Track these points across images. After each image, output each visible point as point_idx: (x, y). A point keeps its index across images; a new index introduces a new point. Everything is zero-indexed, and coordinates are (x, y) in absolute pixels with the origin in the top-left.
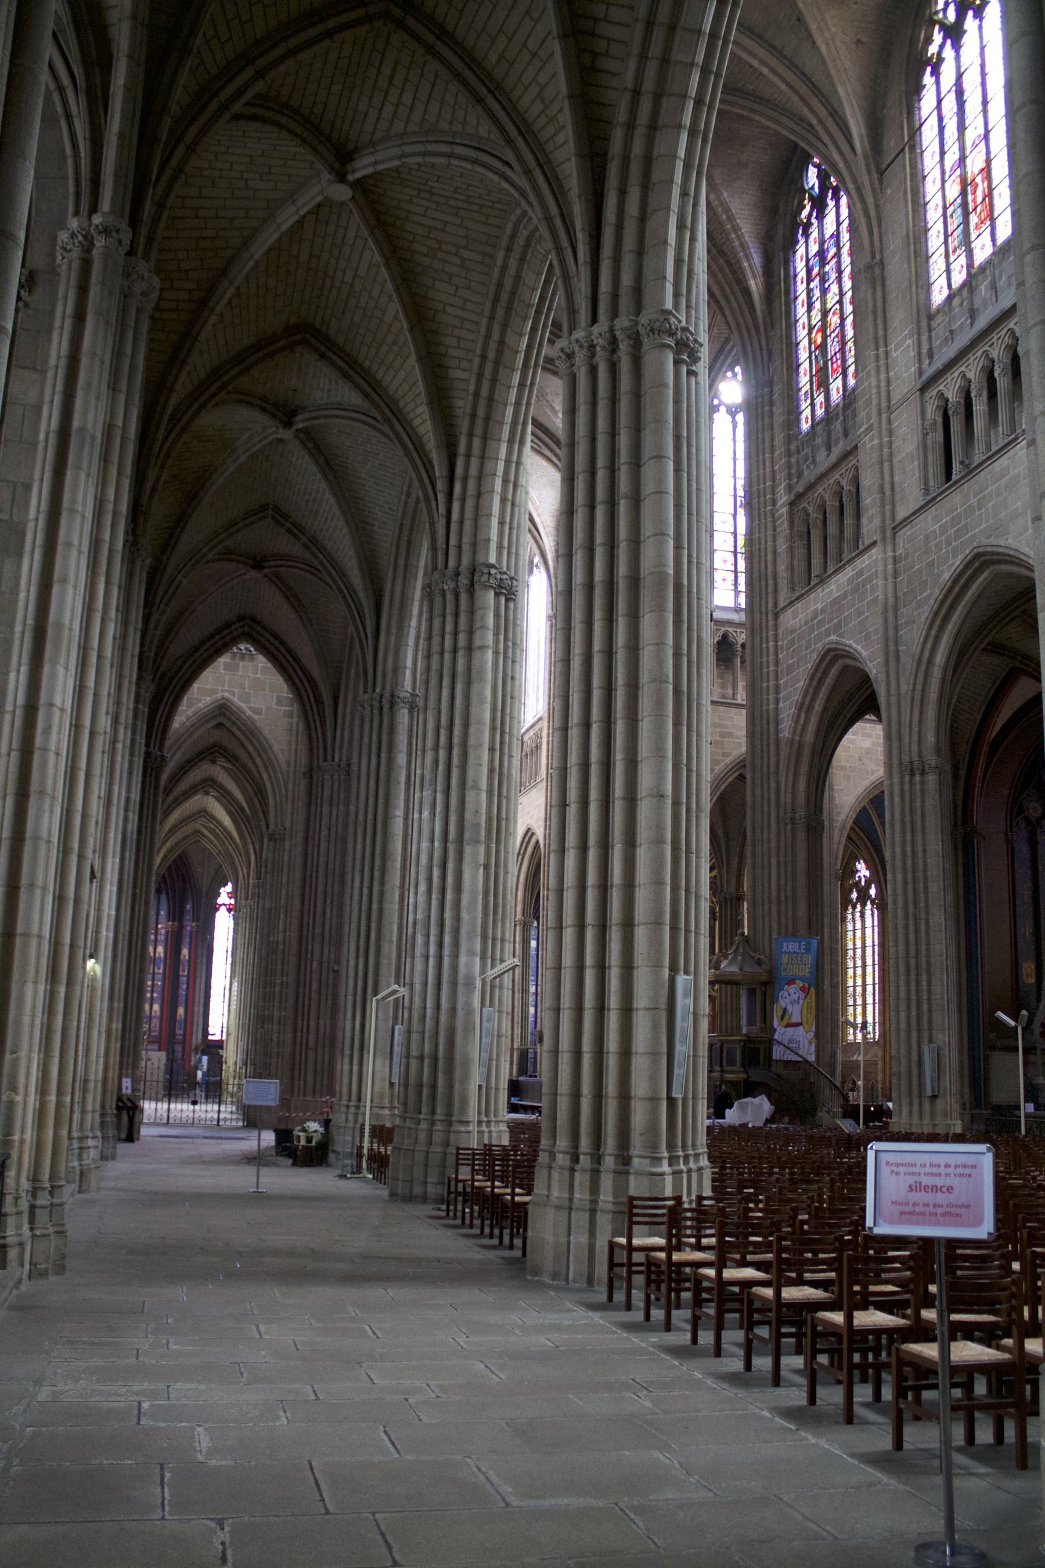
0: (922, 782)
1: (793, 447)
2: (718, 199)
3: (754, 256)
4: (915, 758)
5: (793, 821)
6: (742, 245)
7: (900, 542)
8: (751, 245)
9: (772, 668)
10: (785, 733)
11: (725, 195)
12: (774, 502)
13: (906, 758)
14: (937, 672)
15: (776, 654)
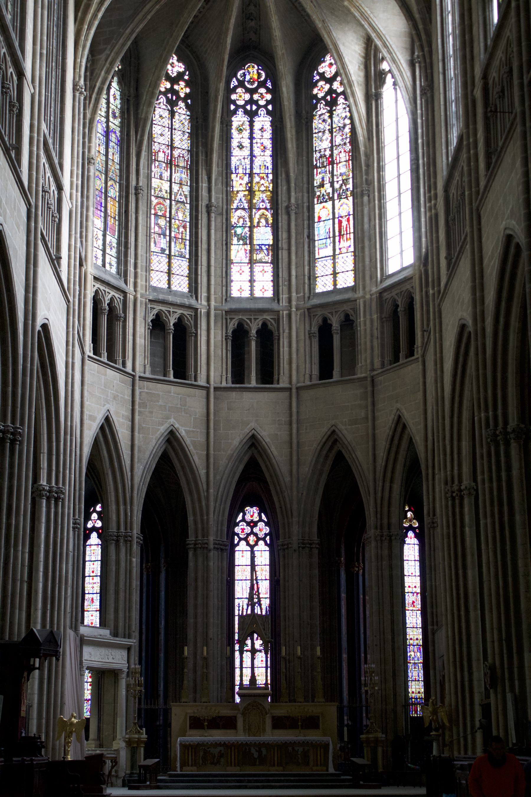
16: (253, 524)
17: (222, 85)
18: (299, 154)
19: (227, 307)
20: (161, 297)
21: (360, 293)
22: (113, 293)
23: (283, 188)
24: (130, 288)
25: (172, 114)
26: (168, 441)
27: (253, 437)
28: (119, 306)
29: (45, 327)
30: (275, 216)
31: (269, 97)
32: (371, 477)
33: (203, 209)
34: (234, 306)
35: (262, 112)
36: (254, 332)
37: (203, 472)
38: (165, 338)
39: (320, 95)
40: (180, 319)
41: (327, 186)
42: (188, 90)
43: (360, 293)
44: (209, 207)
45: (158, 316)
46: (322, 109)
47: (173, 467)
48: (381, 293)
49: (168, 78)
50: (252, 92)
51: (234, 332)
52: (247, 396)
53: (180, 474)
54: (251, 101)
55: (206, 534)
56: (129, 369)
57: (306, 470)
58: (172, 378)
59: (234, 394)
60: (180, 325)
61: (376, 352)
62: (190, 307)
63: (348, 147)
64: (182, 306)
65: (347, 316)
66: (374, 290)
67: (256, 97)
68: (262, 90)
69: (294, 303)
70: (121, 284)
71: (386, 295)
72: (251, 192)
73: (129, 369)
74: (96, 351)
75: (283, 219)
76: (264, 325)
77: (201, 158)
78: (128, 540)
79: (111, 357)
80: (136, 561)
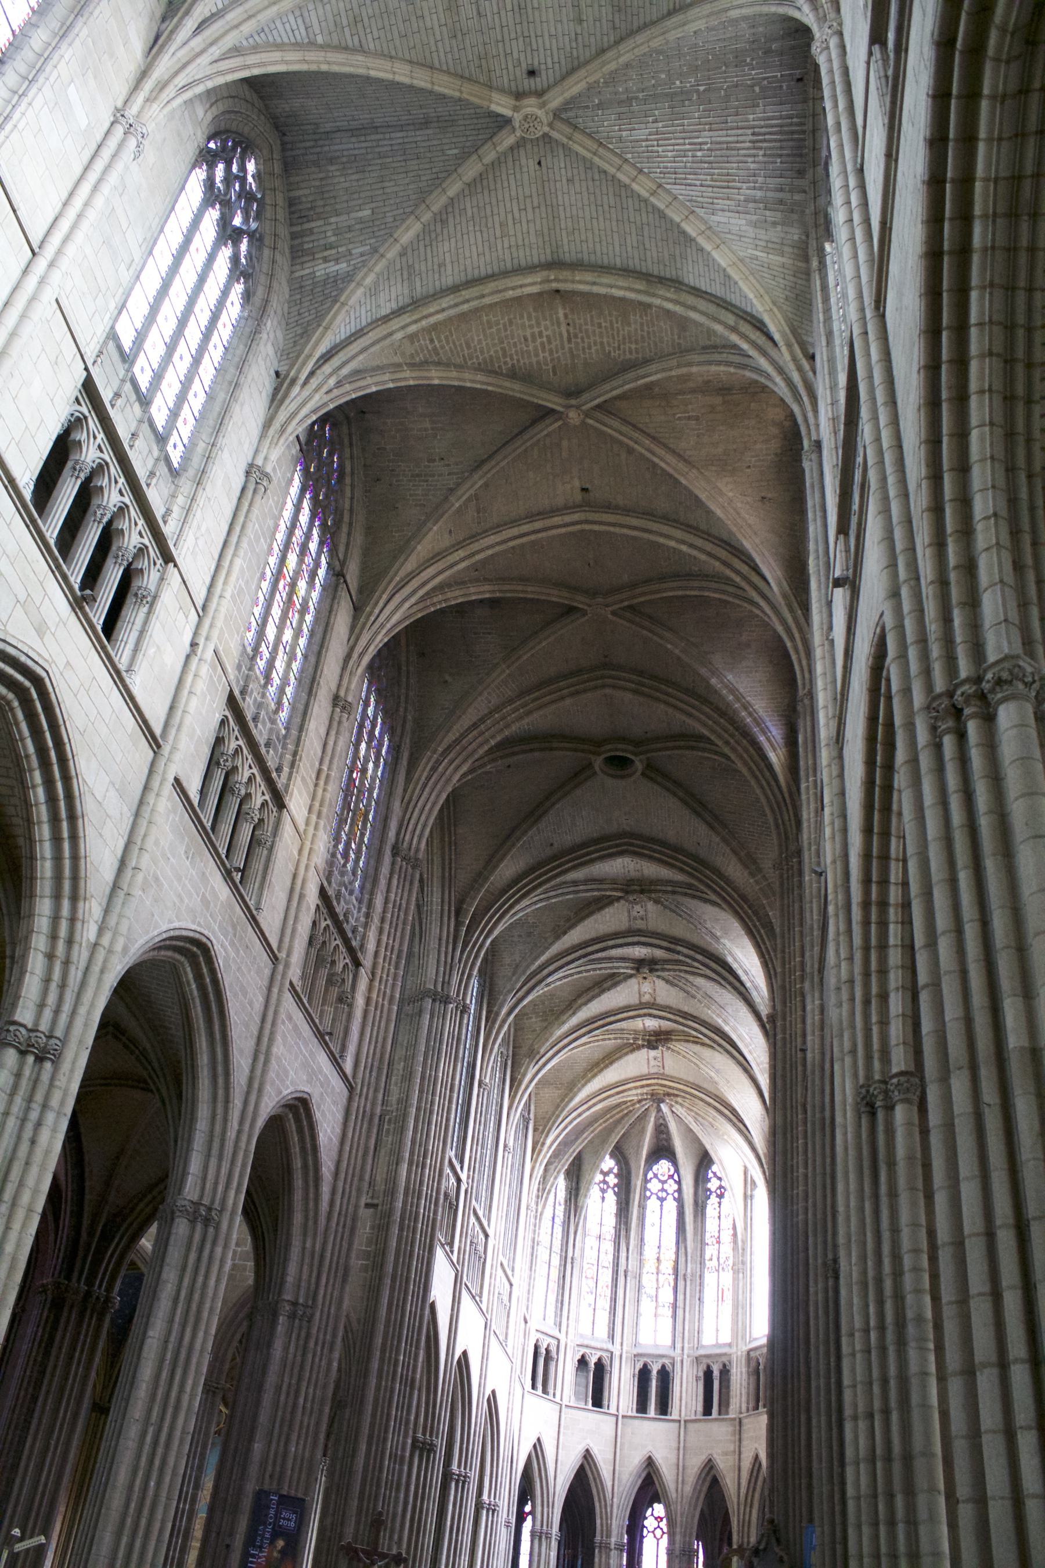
2: (722, 682)
3: (772, 729)
6: (755, 719)
8: (767, 719)
16: (659, 1519)
17: (639, 1183)
18: (695, 1234)
20: (586, 1342)
21: (734, 1350)
22: (550, 1340)
23: (682, 1259)
24: (562, 1337)
25: (603, 1198)
26: (585, 1457)
27: (650, 1458)
29: (493, 1392)
30: (676, 1280)
31: (676, 1187)
32: (735, 1500)
34: (640, 1351)
35: (670, 1198)
36: (654, 1373)
37: (608, 1484)
38: (588, 1371)
39: (713, 1189)
40: (600, 1359)
41: (715, 1262)
42: (616, 1181)
43: (734, 1350)
44: (626, 1272)
45: (583, 1356)
46: (713, 1200)
47: (586, 1475)
48: (749, 1352)
49: (602, 1172)
50: (664, 1182)
51: (640, 1371)
52: (646, 1423)
53: (593, 1485)
54: (663, 1190)
55: (609, 1536)
56: (558, 1399)
57: (688, 1489)
58: (590, 1406)
59: (637, 1422)
60: (600, 1366)
61: (744, 1399)
62: (607, 1351)
63: (731, 1232)
64: (601, 1349)
65: (724, 1365)
66: (745, 1348)
67: (666, 1186)
68: (671, 1181)
69: (686, 1351)
70: (556, 1333)
71: (752, 1354)
72: (658, 1259)
74: (534, 1387)
75: (681, 1283)
76: (663, 1366)
77: (623, 1233)
78: (548, 1537)
79: (545, 1391)
80: (553, 1554)
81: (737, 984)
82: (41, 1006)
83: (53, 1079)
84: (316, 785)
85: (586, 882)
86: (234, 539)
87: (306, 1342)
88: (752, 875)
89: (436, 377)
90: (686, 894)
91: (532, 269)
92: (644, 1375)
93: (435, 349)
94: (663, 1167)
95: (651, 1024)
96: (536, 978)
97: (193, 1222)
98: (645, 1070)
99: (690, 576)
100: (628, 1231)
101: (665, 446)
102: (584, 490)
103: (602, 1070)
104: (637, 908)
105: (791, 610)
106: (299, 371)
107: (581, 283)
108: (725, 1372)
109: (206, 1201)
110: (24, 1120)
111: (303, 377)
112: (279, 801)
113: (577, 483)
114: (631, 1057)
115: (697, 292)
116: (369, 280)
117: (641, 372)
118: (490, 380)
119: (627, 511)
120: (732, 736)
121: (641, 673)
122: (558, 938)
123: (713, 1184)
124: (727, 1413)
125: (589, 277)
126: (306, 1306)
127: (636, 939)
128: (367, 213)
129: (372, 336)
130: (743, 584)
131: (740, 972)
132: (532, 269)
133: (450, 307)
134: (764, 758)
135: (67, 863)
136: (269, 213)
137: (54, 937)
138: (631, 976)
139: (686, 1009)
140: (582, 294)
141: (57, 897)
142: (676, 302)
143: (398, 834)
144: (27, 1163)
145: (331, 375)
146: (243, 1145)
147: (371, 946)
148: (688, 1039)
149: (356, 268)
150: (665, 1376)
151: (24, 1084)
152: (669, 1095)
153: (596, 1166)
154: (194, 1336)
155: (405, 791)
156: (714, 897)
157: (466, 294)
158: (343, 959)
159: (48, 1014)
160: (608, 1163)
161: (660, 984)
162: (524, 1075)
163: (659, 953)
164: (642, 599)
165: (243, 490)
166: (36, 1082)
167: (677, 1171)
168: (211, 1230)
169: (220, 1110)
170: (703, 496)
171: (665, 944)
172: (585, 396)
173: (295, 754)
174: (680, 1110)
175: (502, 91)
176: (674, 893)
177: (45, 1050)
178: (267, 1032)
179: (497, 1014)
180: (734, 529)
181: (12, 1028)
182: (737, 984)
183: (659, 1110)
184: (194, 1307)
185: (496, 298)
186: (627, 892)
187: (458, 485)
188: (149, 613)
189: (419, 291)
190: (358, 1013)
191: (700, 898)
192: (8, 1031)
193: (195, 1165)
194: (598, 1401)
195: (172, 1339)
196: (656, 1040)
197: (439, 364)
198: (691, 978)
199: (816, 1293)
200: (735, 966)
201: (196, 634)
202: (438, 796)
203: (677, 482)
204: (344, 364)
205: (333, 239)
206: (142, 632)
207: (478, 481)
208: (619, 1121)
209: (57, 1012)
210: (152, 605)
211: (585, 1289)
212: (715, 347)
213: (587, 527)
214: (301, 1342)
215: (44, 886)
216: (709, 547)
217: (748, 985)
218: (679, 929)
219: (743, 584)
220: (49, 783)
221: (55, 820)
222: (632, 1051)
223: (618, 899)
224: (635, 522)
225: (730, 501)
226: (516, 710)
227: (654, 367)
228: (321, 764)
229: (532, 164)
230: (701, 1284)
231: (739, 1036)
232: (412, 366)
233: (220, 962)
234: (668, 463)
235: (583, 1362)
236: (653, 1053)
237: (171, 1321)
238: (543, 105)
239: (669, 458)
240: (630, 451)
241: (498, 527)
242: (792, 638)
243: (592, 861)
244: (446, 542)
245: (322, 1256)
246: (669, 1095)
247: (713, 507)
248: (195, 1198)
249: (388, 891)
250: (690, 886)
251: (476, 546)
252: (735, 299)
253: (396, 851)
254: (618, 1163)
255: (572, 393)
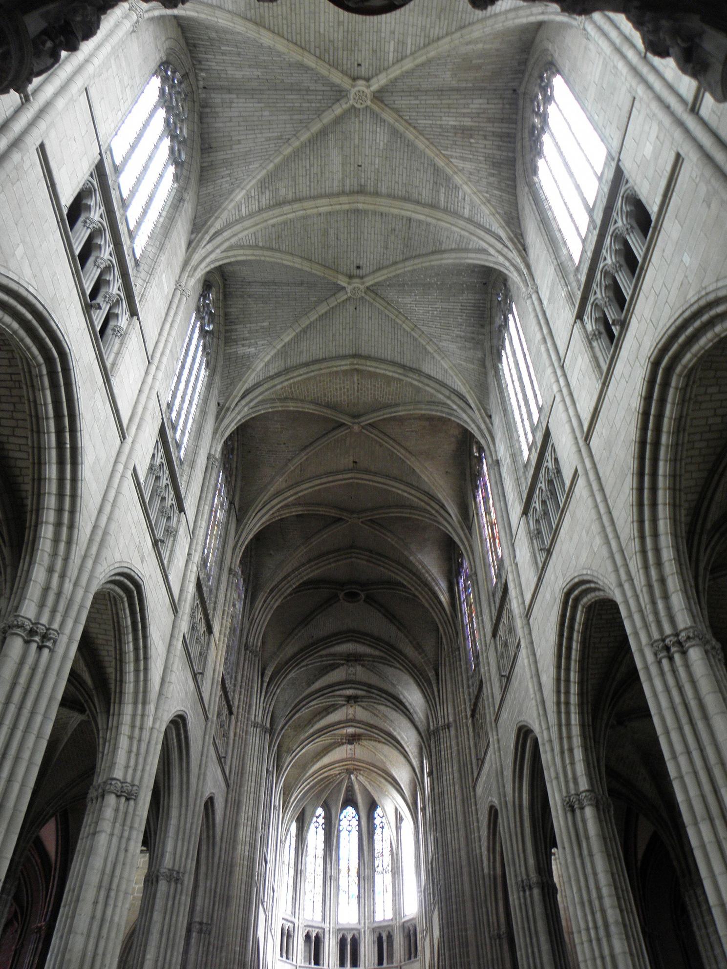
0: (531, 896)
1: (470, 683)
4: (525, 877)
5: (499, 936)
7: (500, 730)
9: (475, 824)
10: (486, 871)
11: (419, 556)
12: (466, 718)
13: (519, 879)
14: (526, 813)
15: (477, 814)
18: (369, 851)
19: (337, 927)
20: (310, 924)
21: (394, 922)
22: (289, 924)
23: (362, 868)
24: (296, 921)
28: (291, 930)
30: (359, 880)
33: (328, 878)
34: (340, 927)
36: (349, 940)
40: (317, 934)
44: (331, 877)
45: (308, 933)
46: (378, 831)
51: (341, 940)
56: (294, 963)
62: (321, 928)
65: (389, 933)
67: (351, 823)
70: (292, 919)
73: (294, 963)
74: (281, 956)
76: (354, 936)
77: (328, 853)
79: (287, 958)
81: (405, 710)
82: (127, 767)
83: (135, 810)
84: (223, 619)
85: (326, 656)
86: (204, 495)
87: (208, 948)
88: (420, 654)
89: (292, 406)
90: (380, 663)
91: (344, 357)
92: (342, 943)
93: (292, 392)
94: (350, 811)
95: (351, 730)
96: (296, 708)
97: (169, 882)
98: (344, 756)
99: (403, 506)
100: (331, 851)
101: (399, 444)
102: (355, 462)
103: (322, 757)
104: (351, 669)
105: (463, 530)
106: (231, 404)
107: (371, 367)
108: (390, 937)
109: (176, 868)
110: (121, 837)
111: (232, 407)
112: (209, 629)
113: (351, 459)
114: (338, 749)
115: (429, 377)
116: (267, 359)
117: (393, 410)
118: (317, 408)
119: (375, 474)
120: (419, 586)
121: (371, 551)
122: (309, 685)
123: (377, 821)
124: (392, 963)
125: (374, 364)
126: (207, 924)
127: (350, 685)
128: (266, 324)
129: (266, 386)
130: (437, 515)
131: (407, 704)
132: (344, 357)
133: (304, 374)
134: (437, 598)
135: (141, 684)
136: (216, 320)
137: (133, 726)
138: (344, 705)
139: (372, 722)
140: (369, 372)
141: (135, 703)
142: (419, 381)
143: (247, 637)
144: (124, 864)
145: (245, 406)
146: (194, 831)
147: (236, 703)
148: (371, 738)
149: (259, 351)
150: (355, 942)
151: (121, 815)
152: (356, 769)
153: (314, 812)
154: (172, 956)
155: (250, 614)
156: (398, 665)
157: (312, 367)
158: (225, 712)
159: (130, 771)
160: (320, 811)
161: (358, 709)
162: (284, 763)
163: (360, 693)
164: (377, 517)
165: (207, 468)
166: (126, 813)
167: (358, 813)
168: (179, 885)
169: (183, 812)
170: (418, 471)
171: (365, 688)
172: (363, 419)
173: (215, 603)
174: (361, 778)
175: (342, 274)
176: (374, 661)
177: (130, 793)
178: (204, 762)
179: (276, 730)
180: (434, 488)
181: (114, 782)
182: (405, 710)
183: (350, 778)
184: (171, 935)
185: (328, 370)
186: (348, 661)
187: (293, 458)
188: (174, 540)
189: (289, 364)
190: (231, 742)
191: (388, 665)
192: (111, 784)
193: (169, 847)
194: (317, 962)
195: (161, 958)
196: (353, 739)
197: (292, 399)
198: (376, 706)
199: (514, 900)
200: (404, 701)
201: (190, 548)
202: (266, 616)
203: (404, 462)
204: (252, 400)
205: (247, 335)
206: (171, 551)
207: (303, 457)
208: (327, 785)
209: (135, 770)
210: (175, 536)
211: (307, 891)
212: (434, 402)
213: (356, 481)
214: (205, 948)
215: (128, 697)
216: (418, 494)
217: (412, 711)
218: (374, 680)
219: (437, 515)
220: (136, 639)
221: (137, 660)
222: (339, 746)
223: (343, 665)
224: (382, 480)
225: (431, 473)
226: (305, 570)
227: (400, 408)
228: (224, 606)
229: (352, 308)
230: (374, 882)
231: (402, 738)
232: (280, 400)
233: (190, 726)
234: (401, 453)
235: (308, 937)
236: (349, 747)
237: (159, 948)
238: (363, 283)
239: (403, 451)
240: (381, 445)
241: (310, 479)
242: (463, 544)
243: (333, 646)
244: (284, 486)
245: (215, 892)
246: (356, 769)
247: (423, 476)
248: (170, 867)
249: (243, 670)
250: (382, 658)
251: (298, 489)
252: (449, 382)
253: (246, 647)
254: (324, 810)
255: (355, 416)
